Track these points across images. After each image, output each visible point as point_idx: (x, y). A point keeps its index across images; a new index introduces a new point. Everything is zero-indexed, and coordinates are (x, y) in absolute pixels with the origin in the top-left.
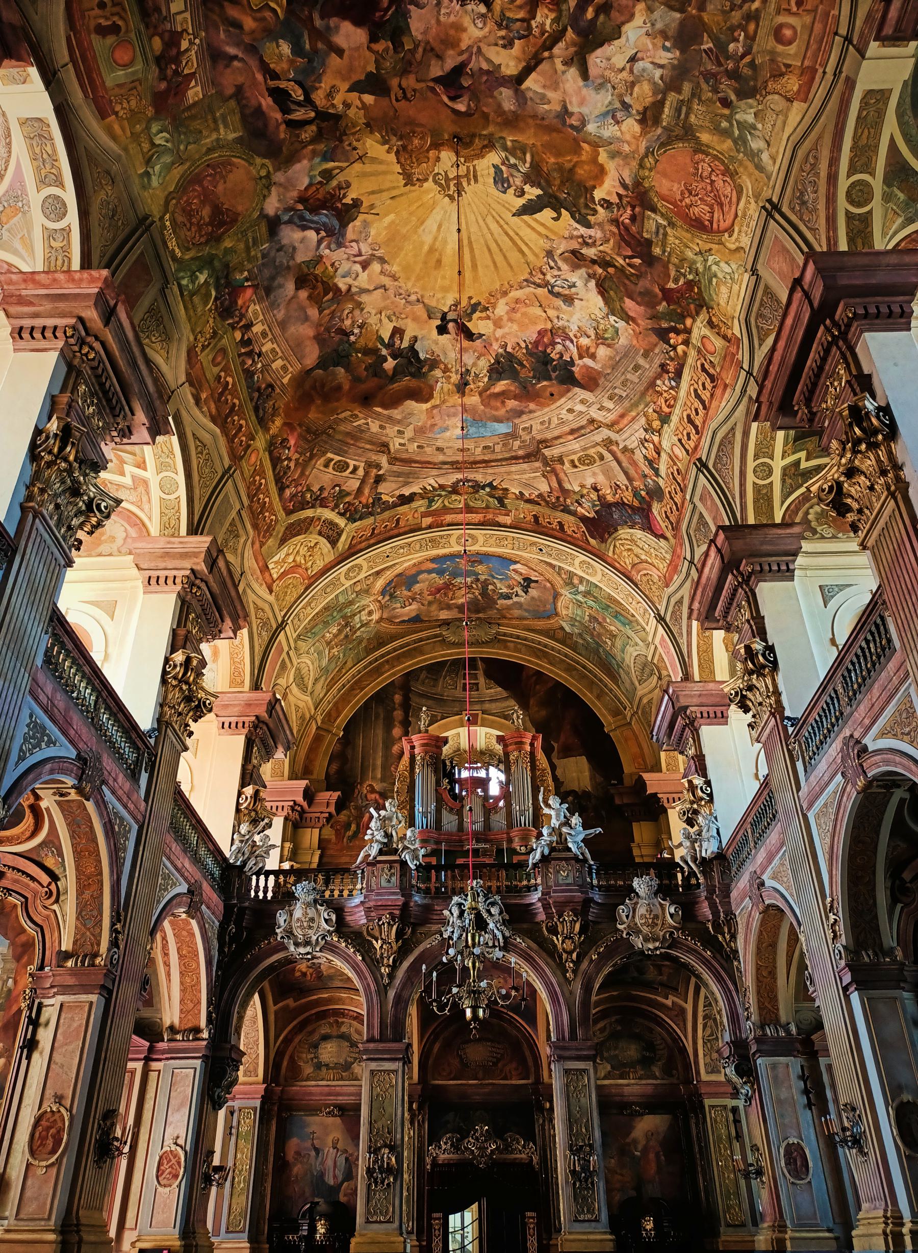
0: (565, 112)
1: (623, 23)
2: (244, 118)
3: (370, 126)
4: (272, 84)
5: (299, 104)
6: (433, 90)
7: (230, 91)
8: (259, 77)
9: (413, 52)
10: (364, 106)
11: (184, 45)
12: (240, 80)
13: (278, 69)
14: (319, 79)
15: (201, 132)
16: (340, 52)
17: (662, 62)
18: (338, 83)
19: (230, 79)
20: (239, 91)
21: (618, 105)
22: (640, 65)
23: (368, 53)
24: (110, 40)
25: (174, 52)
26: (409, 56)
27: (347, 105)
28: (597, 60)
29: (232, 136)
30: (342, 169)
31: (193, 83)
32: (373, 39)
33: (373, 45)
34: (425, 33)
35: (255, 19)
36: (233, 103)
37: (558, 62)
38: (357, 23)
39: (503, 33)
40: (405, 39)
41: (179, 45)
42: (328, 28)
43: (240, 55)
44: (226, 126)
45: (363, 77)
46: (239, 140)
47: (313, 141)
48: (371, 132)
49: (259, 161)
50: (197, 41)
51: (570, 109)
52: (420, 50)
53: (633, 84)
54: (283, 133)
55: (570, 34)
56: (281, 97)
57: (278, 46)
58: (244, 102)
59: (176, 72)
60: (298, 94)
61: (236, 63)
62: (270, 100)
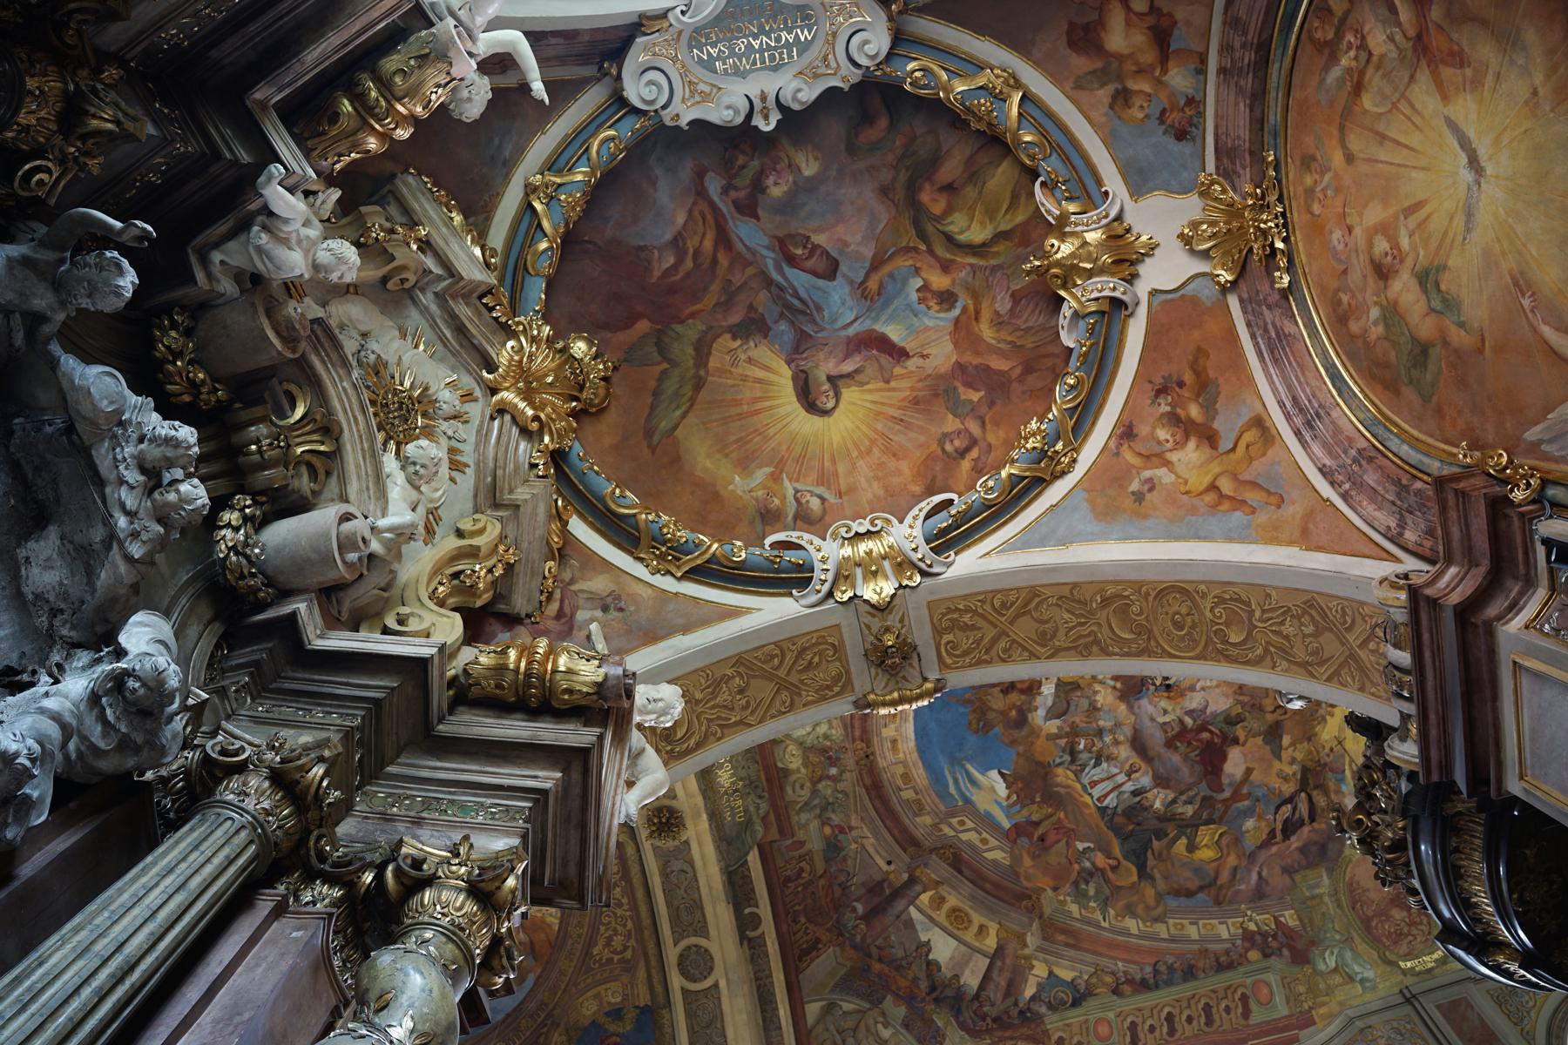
2: (1309, 866)
3: (1310, 737)
4: (1279, 836)
5: (1295, 809)
7: (1287, 880)
8: (1274, 849)
9: (1243, 705)
10: (1293, 744)
11: (1252, 927)
12: (1277, 869)
13: (1266, 831)
14: (1271, 790)
15: (1323, 914)
16: (1249, 771)
18: (1275, 770)
19: (1278, 880)
20: (1288, 871)
23: (1248, 745)
24: (1253, 1005)
25: (1258, 938)
26: (1246, 708)
27: (1293, 761)
29: (1326, 880)
30: (1352, 761)
31: (1282, 919)
32: (1236, 741)
33: (1242, 740)
34: (1227, 696)
35: (1228, 854)
36: (1298, 877)
38: (1224, 758)
40: (1234, 713)
41: (1253, 932)
42: (1230, 784)
43: (1257, 869)
44: (1317, 886)
45: (1268, 748)
46: (1330, 871)
47: (1326, 794)
48: (1315, 735)
49: (1347, 852)
50: (1249, 913)
52: (1241, 698)
56: (1290, 828)
57: (1248, 832)
58: (1296, 865)
59: (1275, 937)
60: (1286, 810)
61: (1264, 873)
62: (1293, 838)
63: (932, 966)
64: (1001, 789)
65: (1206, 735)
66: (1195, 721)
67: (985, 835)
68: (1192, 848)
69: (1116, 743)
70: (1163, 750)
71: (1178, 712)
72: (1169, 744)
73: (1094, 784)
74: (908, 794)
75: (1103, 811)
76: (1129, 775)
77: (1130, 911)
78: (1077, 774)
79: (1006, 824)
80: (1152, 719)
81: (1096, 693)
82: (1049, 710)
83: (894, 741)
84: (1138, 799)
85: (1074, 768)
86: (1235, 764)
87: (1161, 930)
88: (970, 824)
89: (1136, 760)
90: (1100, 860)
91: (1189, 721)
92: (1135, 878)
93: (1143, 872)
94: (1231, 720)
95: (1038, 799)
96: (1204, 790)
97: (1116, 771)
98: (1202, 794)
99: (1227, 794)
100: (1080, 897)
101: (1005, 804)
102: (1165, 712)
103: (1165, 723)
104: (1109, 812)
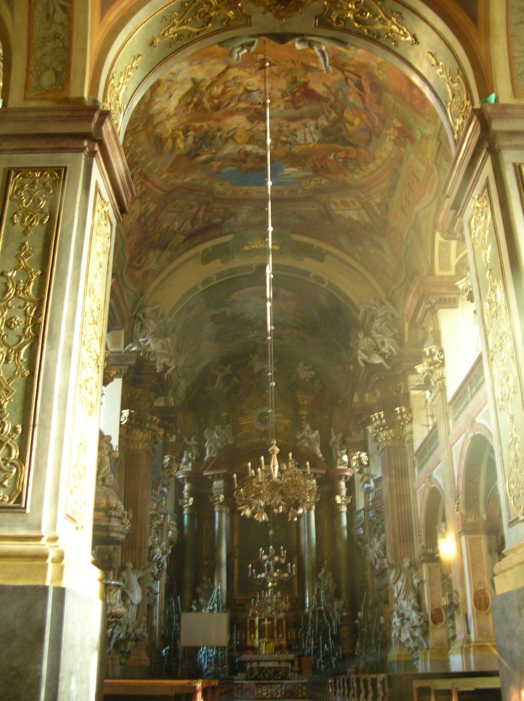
0: (200, 64)
1: (178, 104)
4: (362, 93)
5: (351, 79)
6: (277, 62)
8: (367, 99)
9: (286, 75)
16: (324, 84)
17: (157, 105)
21: (174, 79)
22: (167, 95)
28: (188, 86)
29: (390, 97)
32: (306, 83)
33: (306, 80)
37: (208, 78)
39: (238, 81)
43: (372, 112)
47: (349, 65)
49: (381, 78)
51: (199, 66)
53: (168, 89)
54: (364, 77)
55: (203, 89)
56: (359, 86)
60: (350, 82)
61: (376, 111)
63: (357, 222)
64: (292, 169)
65: (298, 94)
66: (287, 96)
67: (315, 180)
68: (352, 124)
69: (288, 126)
70: (299, 112)
71: (281, 101)
72: (297, 108)
73: (305, 140)
74: (286, 193)
75: (319, 142)
76: (307, 127)
77: (367, 163)
78: (297, 144)
79: (311, 173)
80: (281, 111)
81: (258, 130)
82: (261, 147)
83: (259, 192)
84: (320, 128)
85: (294, 144)
86: (319, 89)
87: (378, 162)
88: (308, 181)
89: (300, 122)
90: (342, 155)
91: (287, 98)
92: (355, 150)
93: (355, 146)
94: (294, 81)
95: (304, 161)
96: (326, 106)
97: (302, 131)
98: (328, 106)
99: (332, 98)
100: (352, 171)
101: (301, 170)
102: (279, 106)
103: (285, 107)
104: (321, 140)
